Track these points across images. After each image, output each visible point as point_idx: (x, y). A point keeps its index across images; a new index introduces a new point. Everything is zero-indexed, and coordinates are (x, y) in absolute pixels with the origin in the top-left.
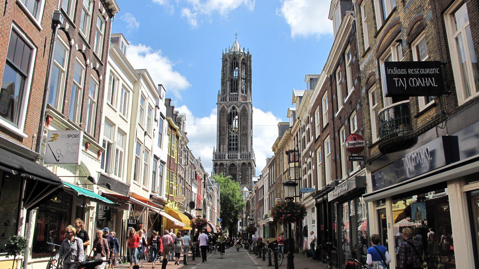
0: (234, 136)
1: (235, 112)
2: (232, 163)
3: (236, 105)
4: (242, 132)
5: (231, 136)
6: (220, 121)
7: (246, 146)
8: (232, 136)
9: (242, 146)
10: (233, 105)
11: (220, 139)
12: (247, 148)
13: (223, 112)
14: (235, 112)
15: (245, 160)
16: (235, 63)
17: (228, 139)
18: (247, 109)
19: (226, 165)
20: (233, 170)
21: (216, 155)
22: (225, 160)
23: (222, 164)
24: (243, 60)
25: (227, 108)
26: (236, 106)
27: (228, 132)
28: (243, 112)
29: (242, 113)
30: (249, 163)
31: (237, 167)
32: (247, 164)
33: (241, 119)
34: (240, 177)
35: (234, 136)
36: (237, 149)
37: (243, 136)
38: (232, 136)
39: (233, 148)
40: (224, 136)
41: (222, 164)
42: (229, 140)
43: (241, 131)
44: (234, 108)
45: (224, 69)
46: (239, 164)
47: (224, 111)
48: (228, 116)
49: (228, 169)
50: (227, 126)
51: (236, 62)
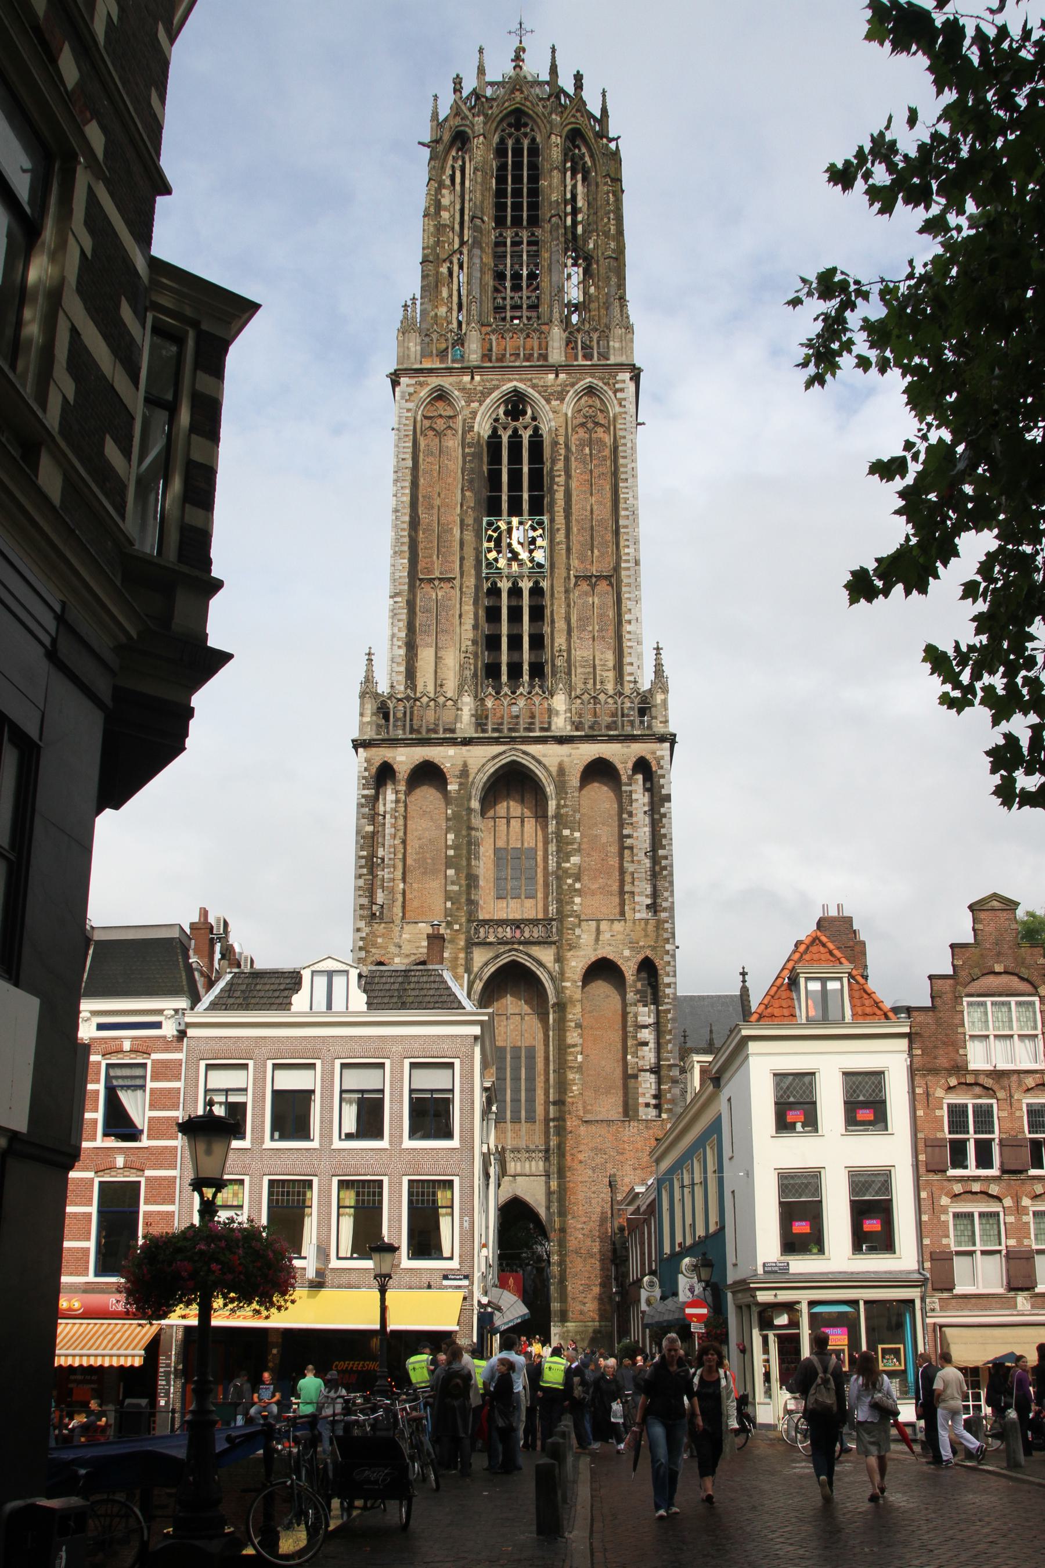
0: (515, 592)
1: (526, 435)
2: (505, 760)
3: (534, 387)
4: (575, 563)
5: (494, 592)
6: (415, 485)
7: (610, 657)
8: (504, 585)
9: (578, 654)
10: (508, 386)
11: (411, 605)
12: (619, 667)
13: (439, 434)
14: (526, 435)
15: (611, 739)
16: (518, 152)
17: (476, 603)
18: (614, 409)
19: (464, 772)
20: (515, 824)
21: (383, 712)
22: (453, 742)
23: (428, 774)
24: (575, 136)
25: (469, 402)
26: (530, 390)
27: (478, 562)
28: (581, 433)
29: (574, 440)
30: (642, 766)
31: (550, 789)
32: (625, 769)
33: (568, 476)
34: (575, 860)
35: (515, 592)
36: (538, 670)
37: (585, 586)
38: (504, 585)
39: (515, 671)
40: (446, 586)
41: (428, 774)
42: (481, 613)
43: (568, 550)
44: (516, 405)
45: (445, 201)
46: (561, 771)
47: (440, 424)
48: (477, 456)
49: (475, 804)
50: (470, 521)
51: (526, 143)
